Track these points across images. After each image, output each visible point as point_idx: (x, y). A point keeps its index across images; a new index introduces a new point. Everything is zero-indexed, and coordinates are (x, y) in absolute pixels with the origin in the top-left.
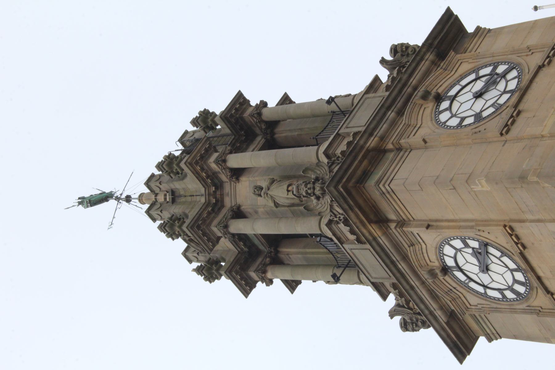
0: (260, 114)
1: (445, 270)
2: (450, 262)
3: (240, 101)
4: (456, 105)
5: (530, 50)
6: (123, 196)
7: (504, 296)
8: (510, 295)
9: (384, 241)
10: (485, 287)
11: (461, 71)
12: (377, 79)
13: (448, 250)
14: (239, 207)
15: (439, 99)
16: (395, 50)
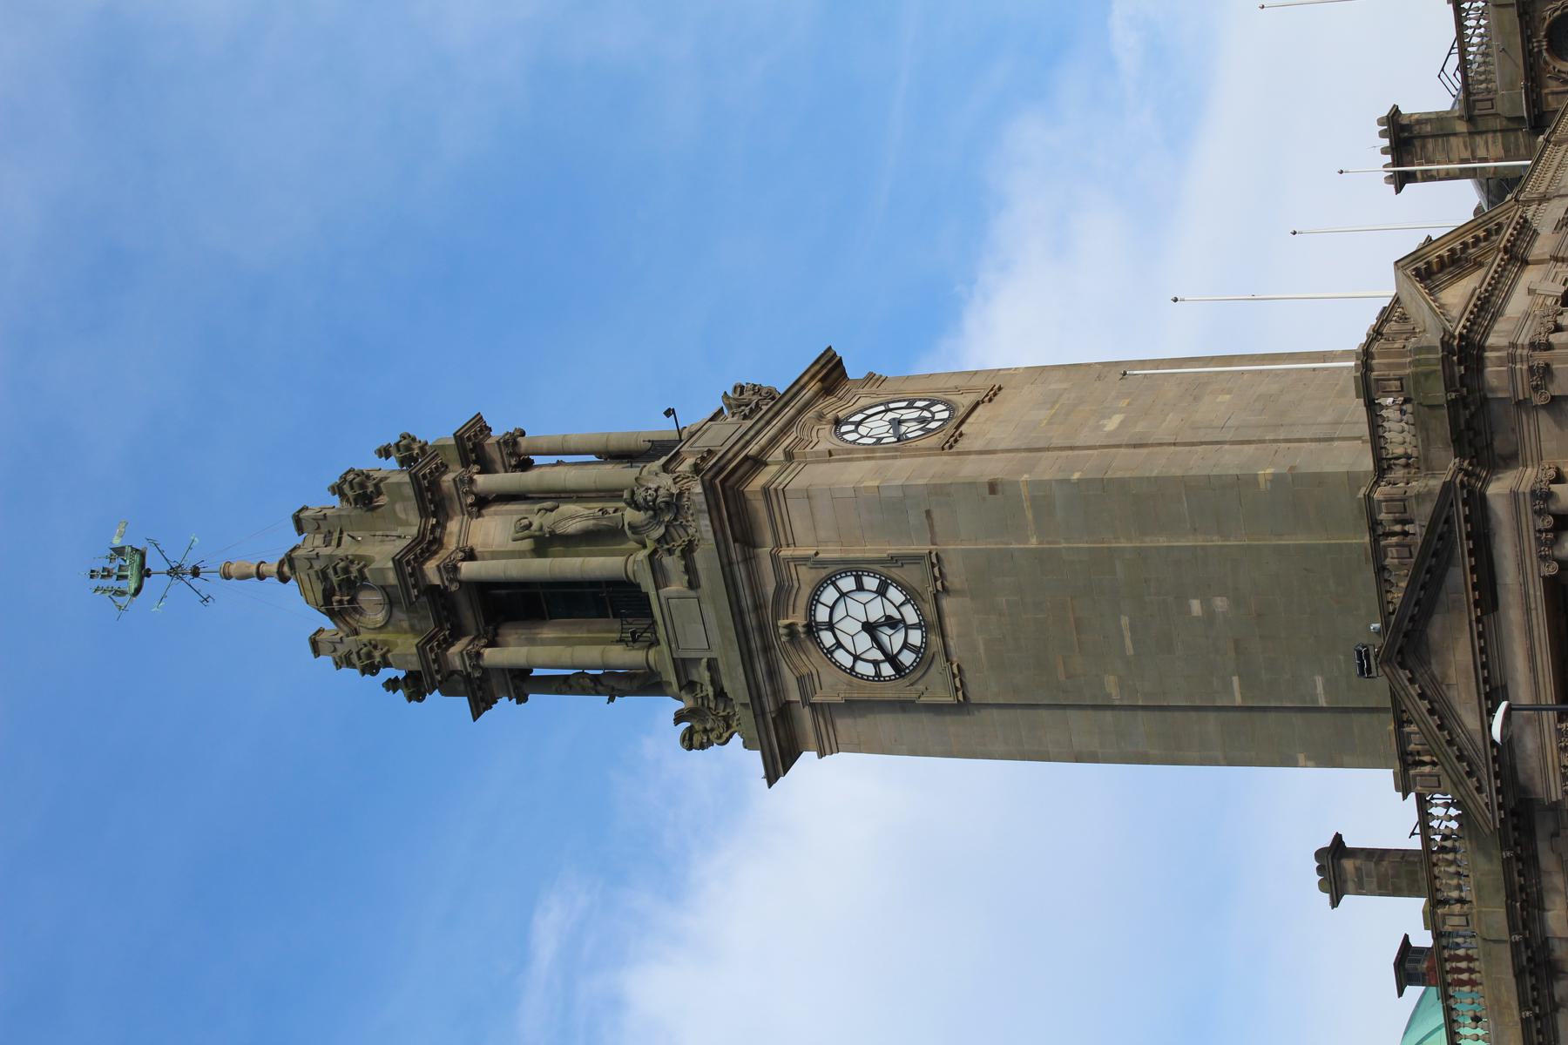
0: (515, 443)
1: (812, 628)
2: (822, 615)
3: (479, 427)
4: (863, 430)
5: (958, 390)
6: (188, 566)
7: (878, 674)
8: (887, 670)
9: (741, 572)
10: (856, 658)
11: (863, 402)
12: (721, 411)
13: (829, 595)
14: (472, 550)
15: (838, 422)
16: (740, 389)
